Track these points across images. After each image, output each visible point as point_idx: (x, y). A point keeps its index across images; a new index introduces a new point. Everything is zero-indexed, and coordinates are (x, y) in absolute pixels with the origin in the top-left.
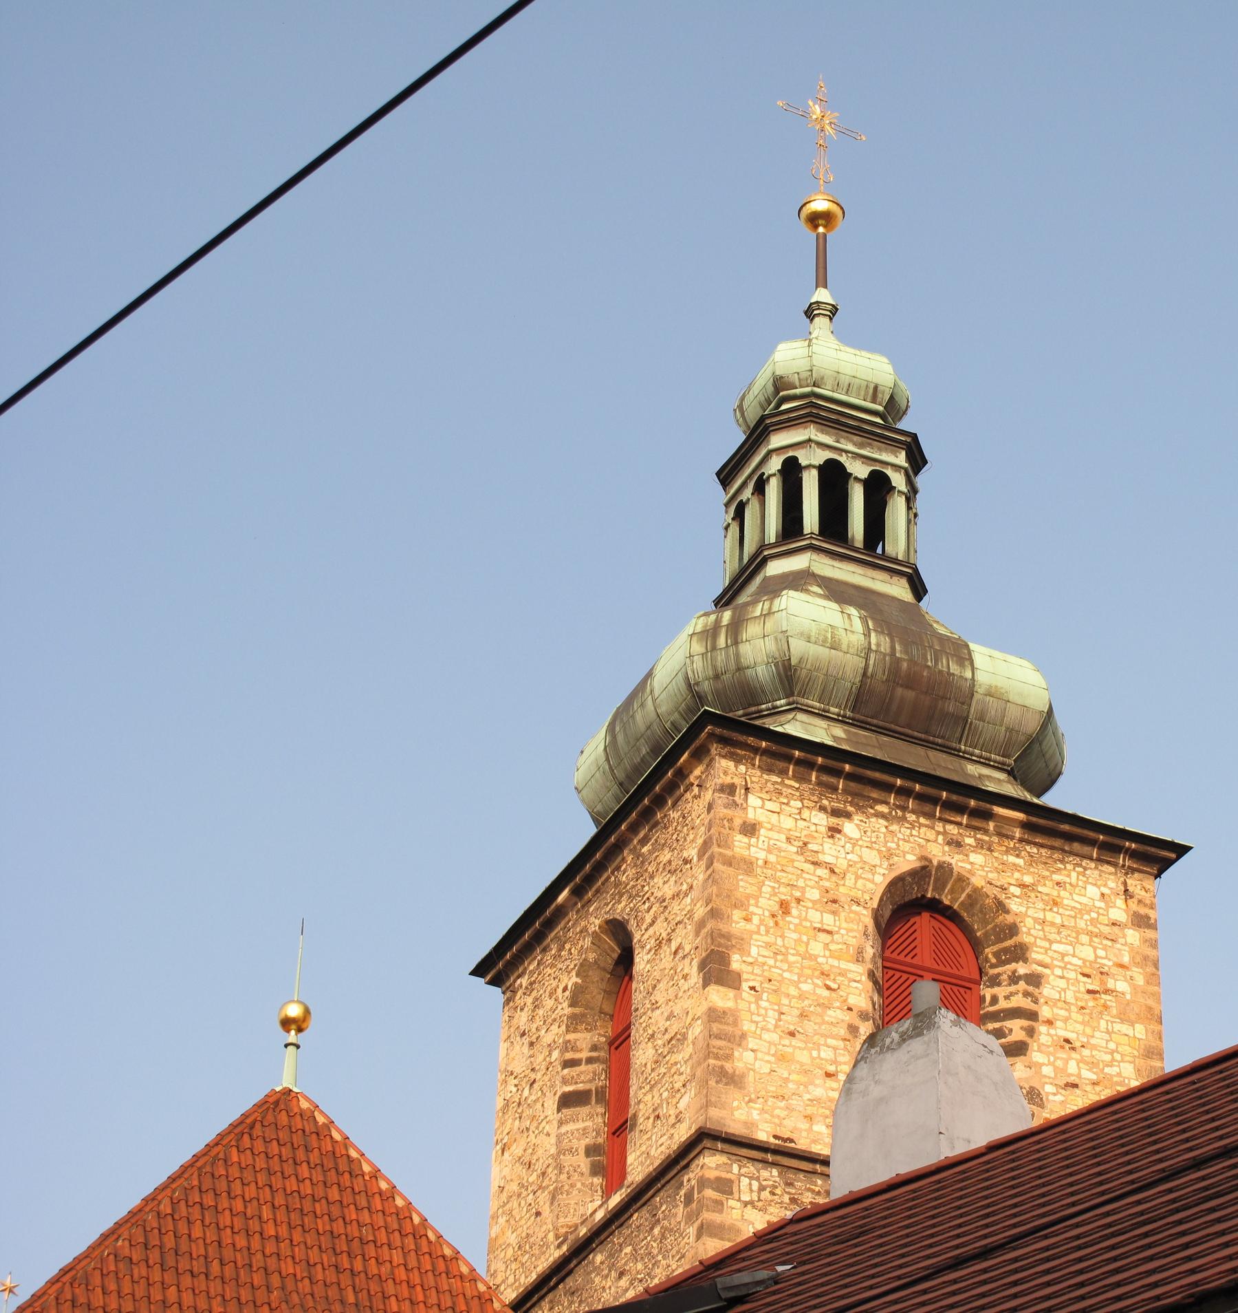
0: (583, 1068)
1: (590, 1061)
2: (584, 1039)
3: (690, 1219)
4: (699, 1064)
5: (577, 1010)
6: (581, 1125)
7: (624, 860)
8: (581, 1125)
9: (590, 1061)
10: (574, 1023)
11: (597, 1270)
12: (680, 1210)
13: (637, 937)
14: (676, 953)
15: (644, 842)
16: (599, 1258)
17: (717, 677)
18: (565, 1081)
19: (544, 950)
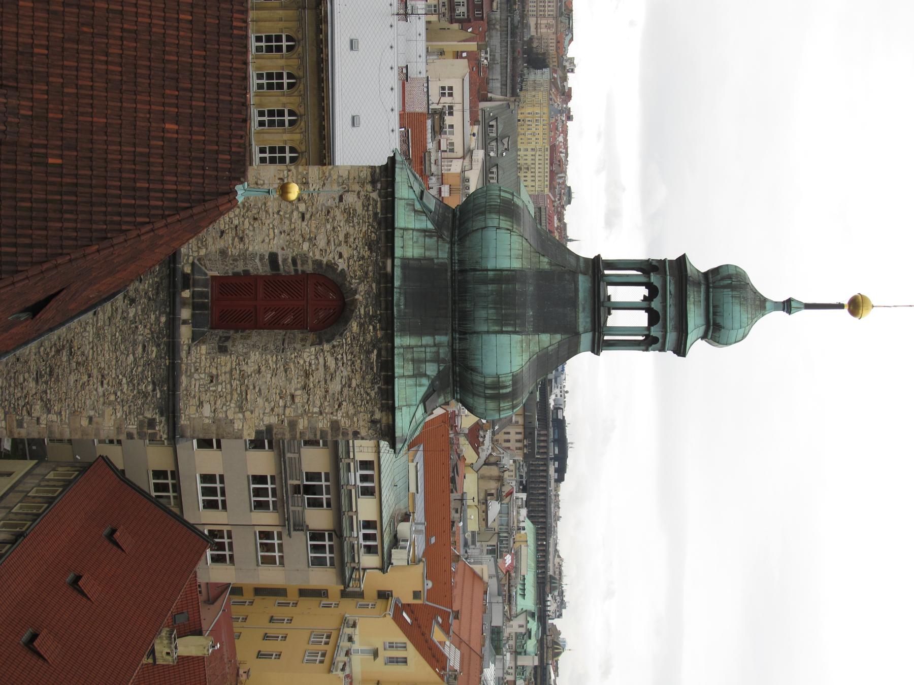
0: (292, 268)
1: (296, 271)
2: (309, 268)
3: (141, 425)
4: (218, 428)
5: (324, 266)
6: (260, 268)
7: (381, 329)
8: (260, 268)
9: (296, 271)
10: (318, 263)
11: (158, 319)
12: (149, 415)
13: (327, 347)
14: (293, 397)
15: (379, 355)
16: (163, 319)
17: (472, 383)
18: (285, 260)
19: (379, 224)
